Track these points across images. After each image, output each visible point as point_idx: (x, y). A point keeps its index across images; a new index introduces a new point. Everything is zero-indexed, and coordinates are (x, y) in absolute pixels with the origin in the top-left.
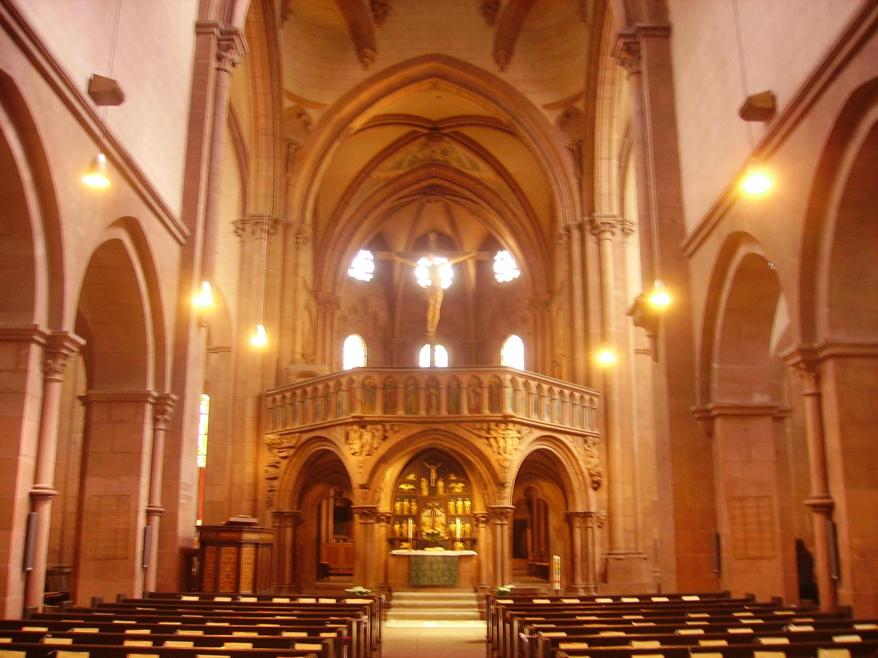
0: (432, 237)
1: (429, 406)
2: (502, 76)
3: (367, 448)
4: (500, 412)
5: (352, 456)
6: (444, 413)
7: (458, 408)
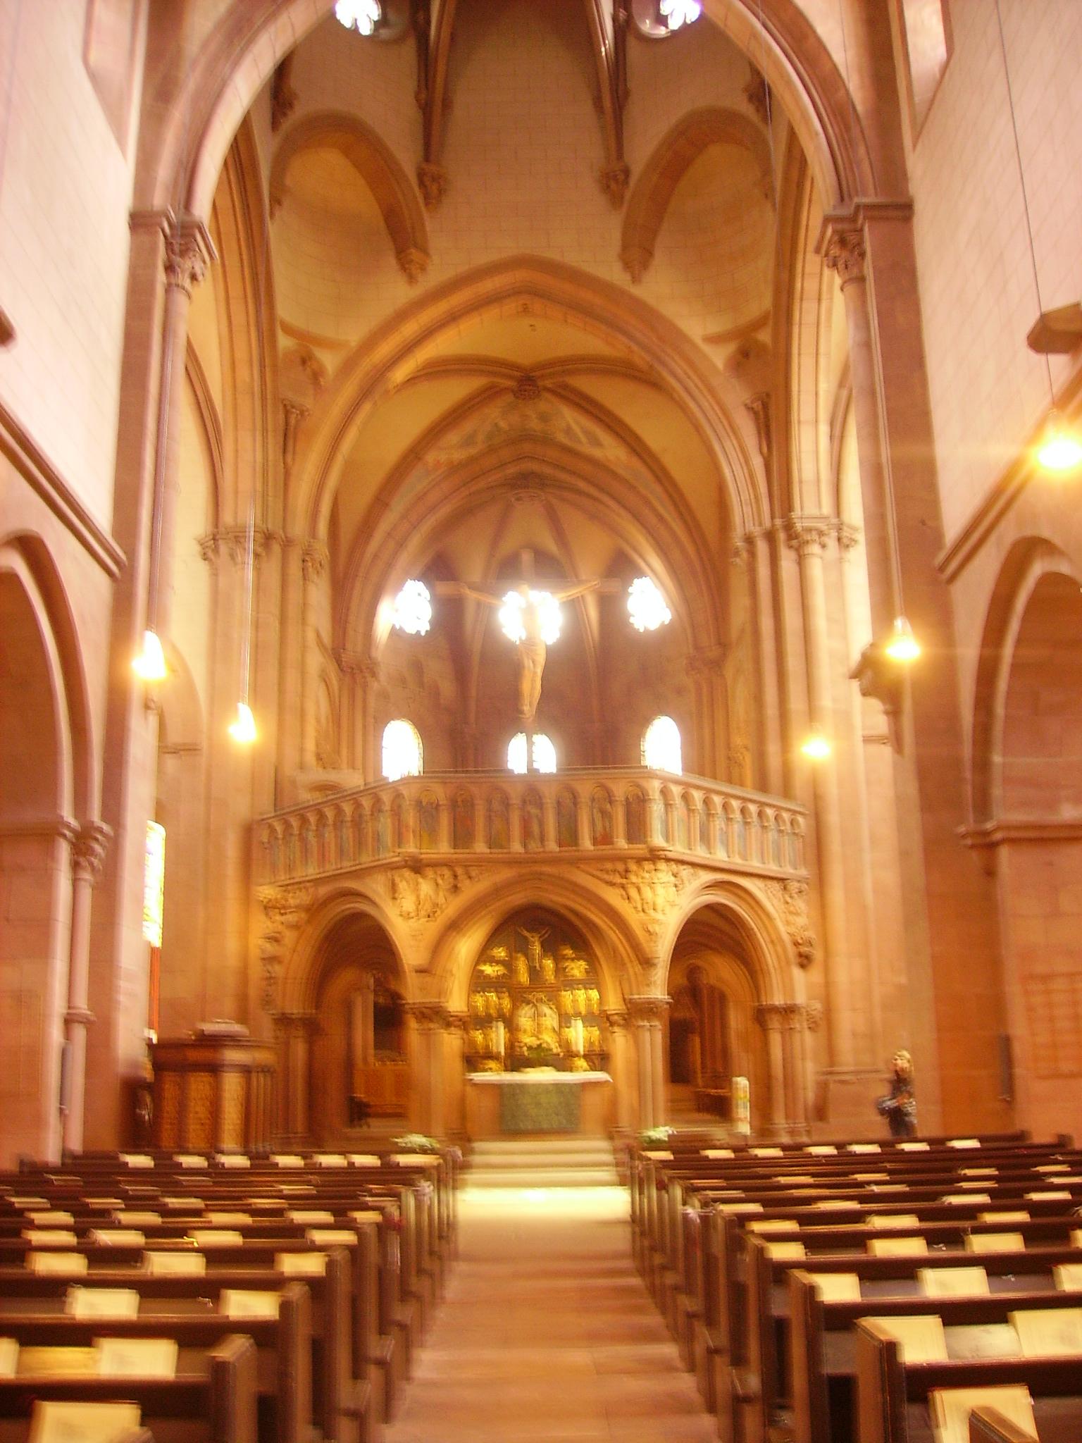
0: (527, 558)
1: (527, 835)
2: (636, 291)
3: (428, 907)
6: (552, 846)
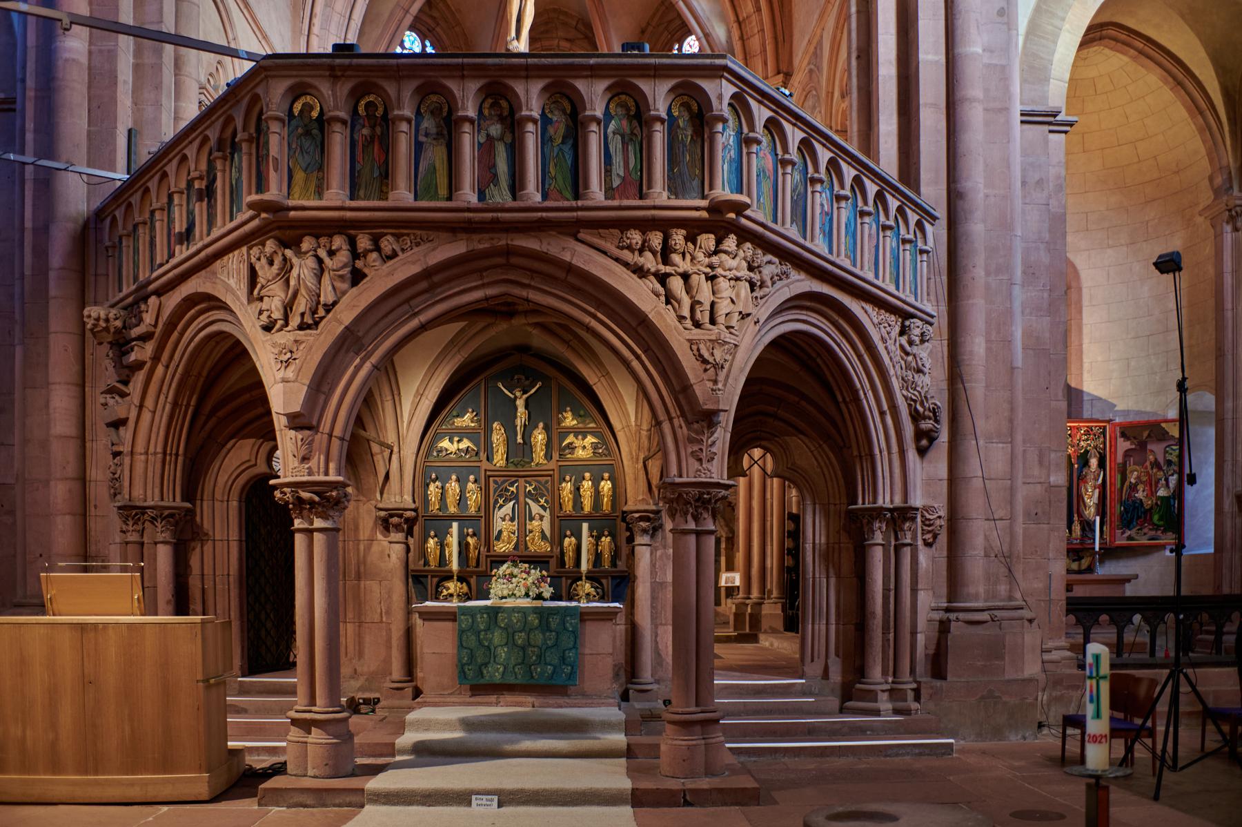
3: (302, 305)
4: (704, 197)
5: (259, 329)
6: (533, 194)
7: (578, 184)
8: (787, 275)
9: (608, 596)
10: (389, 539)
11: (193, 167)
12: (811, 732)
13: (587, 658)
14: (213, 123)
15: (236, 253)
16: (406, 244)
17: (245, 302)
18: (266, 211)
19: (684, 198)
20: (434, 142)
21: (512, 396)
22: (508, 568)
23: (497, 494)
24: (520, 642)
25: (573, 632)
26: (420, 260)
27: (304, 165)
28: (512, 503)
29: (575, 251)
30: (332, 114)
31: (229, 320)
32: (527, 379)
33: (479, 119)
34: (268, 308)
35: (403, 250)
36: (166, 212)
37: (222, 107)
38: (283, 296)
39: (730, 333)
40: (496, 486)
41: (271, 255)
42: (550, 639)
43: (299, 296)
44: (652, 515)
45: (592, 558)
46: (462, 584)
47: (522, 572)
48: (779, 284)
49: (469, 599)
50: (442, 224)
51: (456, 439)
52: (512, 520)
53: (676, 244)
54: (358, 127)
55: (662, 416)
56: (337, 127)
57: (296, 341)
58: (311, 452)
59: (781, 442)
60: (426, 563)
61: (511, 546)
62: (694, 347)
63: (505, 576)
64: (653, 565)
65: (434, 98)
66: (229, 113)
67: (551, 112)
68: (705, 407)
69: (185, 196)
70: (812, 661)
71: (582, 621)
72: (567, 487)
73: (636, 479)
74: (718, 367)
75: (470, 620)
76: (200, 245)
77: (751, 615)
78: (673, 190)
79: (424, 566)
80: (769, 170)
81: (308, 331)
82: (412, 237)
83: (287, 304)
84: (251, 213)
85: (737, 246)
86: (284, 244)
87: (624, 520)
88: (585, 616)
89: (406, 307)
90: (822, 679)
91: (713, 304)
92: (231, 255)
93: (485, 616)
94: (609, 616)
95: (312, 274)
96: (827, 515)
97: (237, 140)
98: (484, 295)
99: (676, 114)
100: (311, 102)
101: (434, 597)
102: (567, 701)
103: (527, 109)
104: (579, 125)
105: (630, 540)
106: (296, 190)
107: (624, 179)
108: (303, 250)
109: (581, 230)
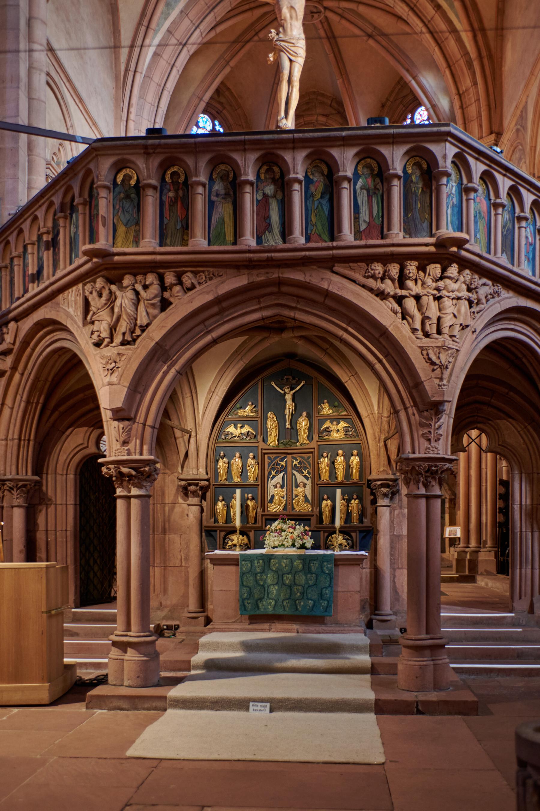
3: (123, 326)
4: (432, 236)
5: (91, 345)
8: (499, 294)
9: (357, 547)
10: (188, 502)
11: (42, 225)
12: (520, 656)
13: (340, 594)
14: (57, 191)
15: (74, 288)
16: (202, 278)
17: (81, 325)
18: (96, 256)
19: (416, 237)
20: (223, 201)
21: (282, 392)
22: (279, 524)
23: (270, 468)
24: (287, 582)
25: (329, 574)
26: (212, 290)
27: (125, 222)
28: (282, 474)
29: (331, 280)
30: (145, 182)
31: (68, 338)
32: (294, 378)
33: (257, 182)
34: (98, 329)
35: (199, 283)
36: (22, 259)
37: (64, 179)
38: (109, 319)
39: (453, 341)
40: (270, 461)
41: (101, 290)
42: (311, 580)
43: (121, 319)
44: (391, 483)
45: (344, 516)
46: (243, 536)
47: (289, 527)
48: (492, 301)
49: (249, 548)
50: (229, 263)
51: (239, 425)
52: (282, 487)
53: (410, 273)
54: (165, 191)
55: (399, 406)
56: (150, 192)
57: (119, 354)
58: (129, 437)
59: (493, 424)
60: (216, 521)
61: (281, 507)
62: (425, 352)
63: (277, 530)
64: (392, 522)
65: (223, 167)
66: (69, 183)
67: (313, 174)
68: (433, 399)
69: (36, 247)
70: (520, 598)
71: (336, 565)
72: (325, 461)
73: (378, 455)
74: (444, 367)
75: (249, 565)
76: (47, 283)
77: (470, 561)
78: (408, 231)
79: (215, 523)
80: (484, 212)
81: (128, 346)
82: (207, 274)
83: (112, 326)
84: (85, 258)
85: (459, 272)
86: (110, 281)
87: (369, 486)
88: (338, 562)
89: (201, 327)
90: (529, 613)
91: (439, 319)
92: (70, 290)
93: (261, 561)
94: (357, 562)
95: (131, 304)
96: (531, 482)
97: (75, 204)
98: (261, 316)
99: (410, 172)
100: (130, 174)
101: (221, 546)
102: (324, 628)
103: (294, 173)
104: (334, 184)
105: (374, 502)
106: (119, 240)
107: (369, 224)
108: (124, 285)
109: (336, 265)
